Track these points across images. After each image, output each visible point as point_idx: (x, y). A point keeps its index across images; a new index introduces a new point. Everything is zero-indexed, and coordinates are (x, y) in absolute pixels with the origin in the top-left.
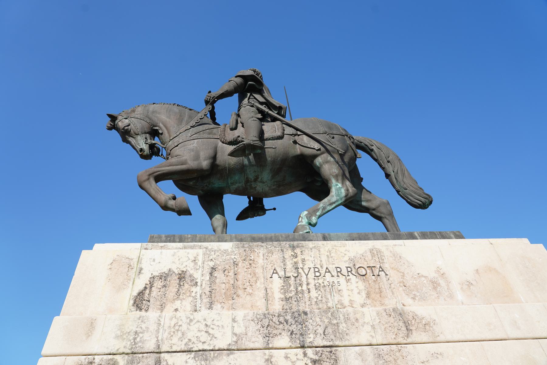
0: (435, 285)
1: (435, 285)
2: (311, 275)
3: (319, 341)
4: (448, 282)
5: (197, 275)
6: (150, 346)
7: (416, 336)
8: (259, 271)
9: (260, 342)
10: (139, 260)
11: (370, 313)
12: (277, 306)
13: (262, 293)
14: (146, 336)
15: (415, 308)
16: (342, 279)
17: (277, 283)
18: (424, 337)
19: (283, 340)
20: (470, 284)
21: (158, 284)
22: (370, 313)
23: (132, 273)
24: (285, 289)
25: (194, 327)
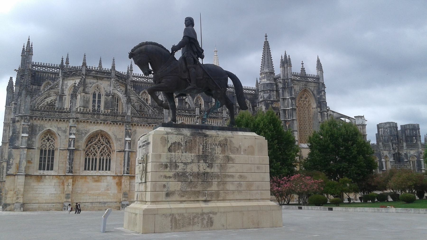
0: (238, 149)
1: (238, 149)
2: (209, 145)
3: (209, 162)
4: (241, 149)
5: (182, 143)
6: (174, 161)
7: (230, 162)
8: (197, 143)
9: (197, 161)
10: (168, 138)
11: (221, 156)
12: (201, 153)
13: (197, 149)
14: (173, 159)
15: (232, 156)
16: (216, 147)
17: (201, 147)
18: (231, 162)
19: (202, 161)
20: (245, 150)
21: (173, 145)
22: (221, 156)
23: (166, 142)
24: (203, 149)
25: (183, 157)
